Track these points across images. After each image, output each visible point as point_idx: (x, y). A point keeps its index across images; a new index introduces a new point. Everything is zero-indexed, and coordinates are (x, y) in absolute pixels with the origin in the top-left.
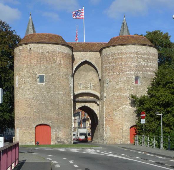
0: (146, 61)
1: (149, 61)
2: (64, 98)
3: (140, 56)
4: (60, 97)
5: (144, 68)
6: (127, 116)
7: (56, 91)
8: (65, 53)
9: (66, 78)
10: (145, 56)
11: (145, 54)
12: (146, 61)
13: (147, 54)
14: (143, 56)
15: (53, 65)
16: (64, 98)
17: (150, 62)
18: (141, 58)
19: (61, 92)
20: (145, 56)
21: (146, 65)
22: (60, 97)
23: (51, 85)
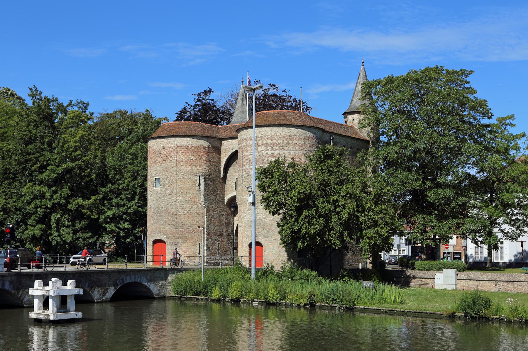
0: (270, 148)
1: (274, 148)
2: (185, 205)
3: (261, 142)
4: (178, 205)
5: (266, 159)
6: (246, 228)
7: (173, 197)
8: (188, 146)
9: (190, 179)
10: (269, 142)
11: (268, 139)
12: (270, 148)
13: (272, 138)
14: (265, 142)
15: (170, 164)
16: (185, 205)
17: (279, 150)
18: (262, 144)
19: (181, 198)
20: (269, 142)
21: (270, 153)
22: (178, 205)
23: (166, 189)
